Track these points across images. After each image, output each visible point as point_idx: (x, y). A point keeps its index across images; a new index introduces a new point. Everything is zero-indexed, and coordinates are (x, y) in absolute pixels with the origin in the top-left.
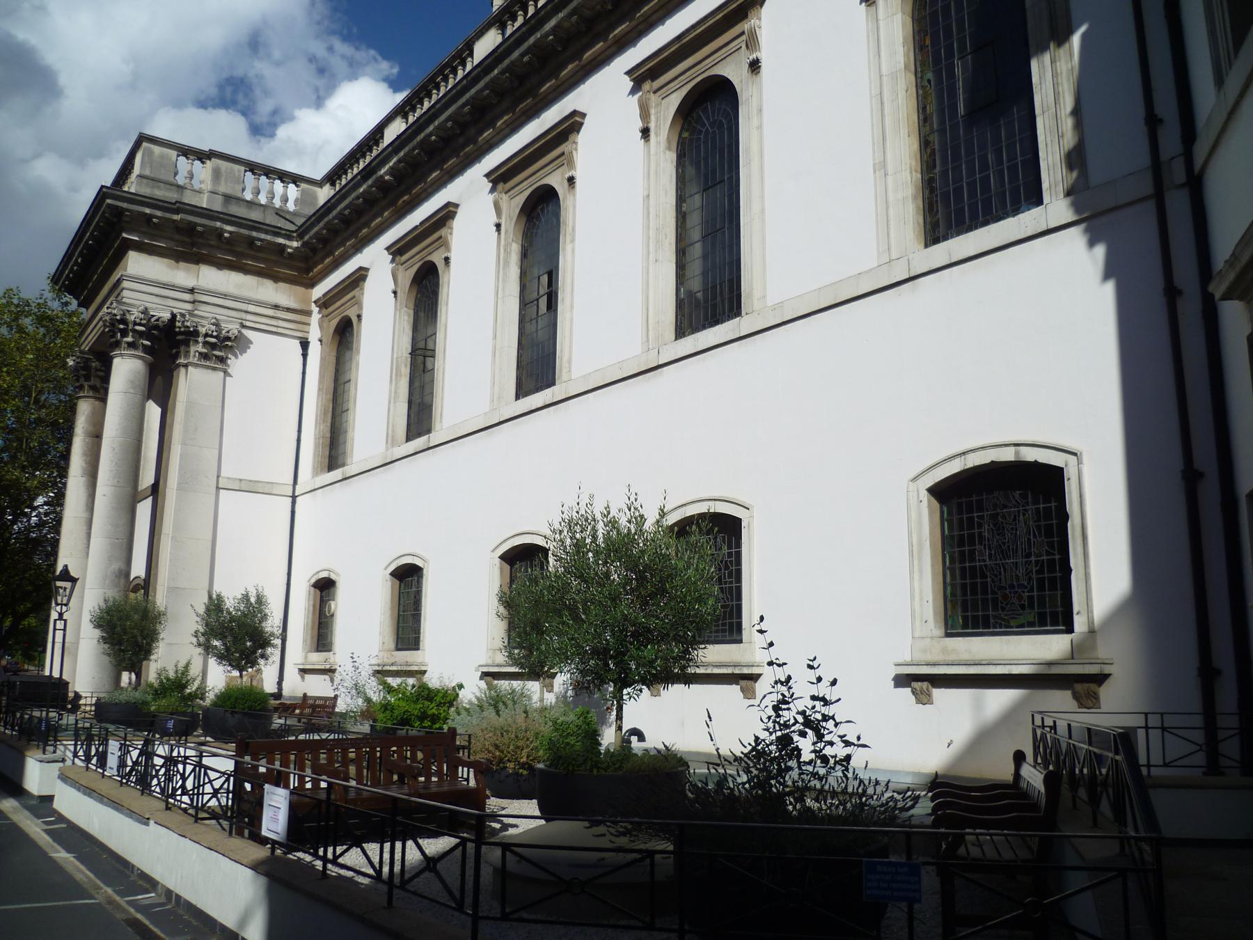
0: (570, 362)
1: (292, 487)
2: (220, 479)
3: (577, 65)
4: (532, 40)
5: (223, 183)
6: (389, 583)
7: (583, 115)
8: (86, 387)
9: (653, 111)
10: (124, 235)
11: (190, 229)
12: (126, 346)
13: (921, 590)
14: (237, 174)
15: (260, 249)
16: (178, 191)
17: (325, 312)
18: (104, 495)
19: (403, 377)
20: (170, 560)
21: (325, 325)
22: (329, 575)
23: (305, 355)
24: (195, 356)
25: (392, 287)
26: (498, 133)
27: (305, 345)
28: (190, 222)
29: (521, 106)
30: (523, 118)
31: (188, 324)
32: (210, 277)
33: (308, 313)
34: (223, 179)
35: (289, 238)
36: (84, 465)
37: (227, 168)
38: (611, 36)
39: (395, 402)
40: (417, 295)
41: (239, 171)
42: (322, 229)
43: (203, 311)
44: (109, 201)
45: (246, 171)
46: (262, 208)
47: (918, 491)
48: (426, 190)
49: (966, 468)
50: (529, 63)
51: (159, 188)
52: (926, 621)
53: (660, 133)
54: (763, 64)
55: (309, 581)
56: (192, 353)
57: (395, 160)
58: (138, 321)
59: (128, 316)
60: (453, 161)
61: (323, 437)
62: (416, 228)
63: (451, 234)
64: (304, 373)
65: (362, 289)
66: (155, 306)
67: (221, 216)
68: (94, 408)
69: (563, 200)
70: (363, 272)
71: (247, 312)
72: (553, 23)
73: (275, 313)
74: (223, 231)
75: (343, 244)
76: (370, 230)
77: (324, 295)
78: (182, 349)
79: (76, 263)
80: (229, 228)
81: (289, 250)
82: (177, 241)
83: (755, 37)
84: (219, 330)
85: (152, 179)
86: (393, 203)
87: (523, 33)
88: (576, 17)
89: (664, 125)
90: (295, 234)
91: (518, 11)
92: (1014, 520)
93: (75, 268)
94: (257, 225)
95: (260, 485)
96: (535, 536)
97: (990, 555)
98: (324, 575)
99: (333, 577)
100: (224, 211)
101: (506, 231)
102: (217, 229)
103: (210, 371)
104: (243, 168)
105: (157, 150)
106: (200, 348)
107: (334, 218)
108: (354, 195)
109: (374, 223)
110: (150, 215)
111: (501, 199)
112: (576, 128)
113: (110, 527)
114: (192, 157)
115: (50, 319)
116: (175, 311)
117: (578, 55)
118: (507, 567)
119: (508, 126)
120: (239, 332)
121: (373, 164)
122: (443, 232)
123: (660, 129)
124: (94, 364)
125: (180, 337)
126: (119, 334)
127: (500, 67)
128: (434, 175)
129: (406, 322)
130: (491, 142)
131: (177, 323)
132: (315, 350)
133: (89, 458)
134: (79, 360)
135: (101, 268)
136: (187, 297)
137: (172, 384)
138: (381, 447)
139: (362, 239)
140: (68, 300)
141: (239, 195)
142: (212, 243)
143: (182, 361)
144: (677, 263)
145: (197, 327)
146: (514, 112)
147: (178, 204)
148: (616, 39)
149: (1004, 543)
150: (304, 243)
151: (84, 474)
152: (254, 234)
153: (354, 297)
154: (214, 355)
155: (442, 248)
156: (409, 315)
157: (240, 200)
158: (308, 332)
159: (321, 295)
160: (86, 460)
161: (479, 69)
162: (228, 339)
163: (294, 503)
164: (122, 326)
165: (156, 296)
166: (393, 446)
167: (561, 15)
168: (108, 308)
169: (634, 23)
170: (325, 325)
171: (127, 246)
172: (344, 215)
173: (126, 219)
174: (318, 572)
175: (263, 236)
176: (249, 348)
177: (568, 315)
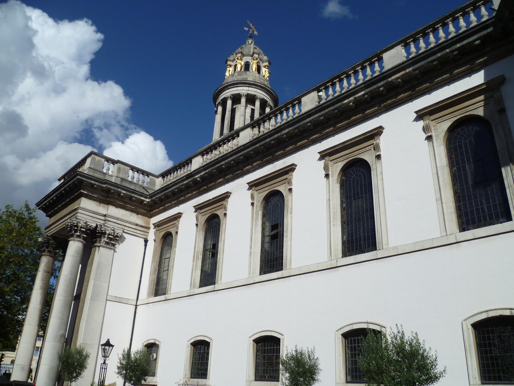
0: (291, 261)
1: (136, 301)
2: (108, 296)
3: (294, 147)
4: (276, 136)
5: (121, 173)
6: (190, 348)
7: (296, 166)
8: (46, 251)
9: (330, 168)
10: (82, 191)
11: (108, 191)
12: (76, 236)
13: (472, 365)
14: (127, 170)
15: (134, 201)
16: (103, 175)
17: (157, 228)
18: (60, 300)
19: (199, 259)
20: (84, 331)
21: (157, 234)
22: (155, 342)
23: (146, 246)
24: (103, 243)
25: (195, 222)
26: (253, 168)
27: (146, 241)
28: (109, 188)
29: (266, 159)
30: (266, 163)
31: (103, 229)
32: (113, 211)
33: (149, 228)
34: (121, 172)
35: (146, 197)
36: (41, 285)
37: (123, 168)
38: (311, 138)
39: (195, 270)
40: (206, 226)
41: (127, 169)
42: (162, 195)
43: (109, 224)
44: (79, 177)
45: (130, 169)
46: (135, 184)
47: (467, 324)
48: (215, 185)
49: (488, 317)
50: (273, 144)
51: (96, 173)
52: (475, 378)
53: (334, 176)
54: (382, 156)
55: (143, 344)
56: (102, 241)
57: (203, 173)
58: (83, 226)
59: (79, 224)
60: (230, 175)
61: (153, 281)
62: (210, 200)
63: (227, 204)
64: (145, 253)
65: (179, 221)
66: (90, 221)
67: (121, 187)
68: (49, 260)
69: (286, 197)
70: (180, 215)
71: (125, 226)
72: (287, 131)
73: (136, 227)
75: (170, 202)
76: (185, 198)
78: (98, 239)
79: (52, 199)
81: (145, 202)
82: (102, 195)
83: (378, 147)
84: (114, 233)
85: (94, 169)
86: (199, 189)
87: (273, 133)
88: (297, 130)
89: (335, 173)
90: (148, 196)
91: (261, 123)
92: (509, 338)
93: (51, 201)
94: (135, 191)
95: (123, 299)
96: (272, 332)
97: (499, 352)
98: (153, 341)
99: (157, 342)
100: (121, 184)
101: (256, 206)
102: (119, 191)
103: (109, 249)
104: (129, 168)
105: (97, 158)
106: (106, 239)
107: (169, 192)
108: (180, 184)
109: (187, 196)
110: (94, 184)
111: (254, 193)
113: (61, 314)
114: (110, 162)
115: (23, 219)
116: (98, 223)
117: (295, 143)
118: (255, 345)
119: (258, 165)
120: (122, 234)
121: (193, 173)
122: (223, 202)
123: (334, 175)
124: (51, 241)
125: (97, 234)
126: (73, 231)
128: (220, 180)
129: (202, 237)
130: (249, 170)
131: (98, 228)
132: (151, 244)
133: (44, 282)
134: (46, 239)
135: (65, 202)
136: (103, 218)
137: (91, 253)
139: (180, 201)
140: (32, 212)
141: (127, 179)
142: (115, 197)
143: (98, 244)
144: (341, 226)
145: (106, 231)
147: (105, 181)
148: (312, 139)
149: (505, 347)
150: (152, 200)
151: (41, 289)
152: (133, 195)
153: (175, 224)
154: (111, 243)
155: (222, 209)
156: (203, 235)
157: (127, 181)
158: (148, 236)
159: (157, 222)
160: (42, 282)
161: (250, 143)
162: (117, 236)
163: (136, 308)
164: (76, 228)
165: (91, 216)
166: (194, 288)
167: (290, 129)
168: (70, 220)
169: (321, 135)
170: (157, 234)
171: (81, 195)
172: (175, 191)
173: (84, 185)
174: (149, 340)
175: (136, 196)
176: (124, 241)
177: (289, 243)
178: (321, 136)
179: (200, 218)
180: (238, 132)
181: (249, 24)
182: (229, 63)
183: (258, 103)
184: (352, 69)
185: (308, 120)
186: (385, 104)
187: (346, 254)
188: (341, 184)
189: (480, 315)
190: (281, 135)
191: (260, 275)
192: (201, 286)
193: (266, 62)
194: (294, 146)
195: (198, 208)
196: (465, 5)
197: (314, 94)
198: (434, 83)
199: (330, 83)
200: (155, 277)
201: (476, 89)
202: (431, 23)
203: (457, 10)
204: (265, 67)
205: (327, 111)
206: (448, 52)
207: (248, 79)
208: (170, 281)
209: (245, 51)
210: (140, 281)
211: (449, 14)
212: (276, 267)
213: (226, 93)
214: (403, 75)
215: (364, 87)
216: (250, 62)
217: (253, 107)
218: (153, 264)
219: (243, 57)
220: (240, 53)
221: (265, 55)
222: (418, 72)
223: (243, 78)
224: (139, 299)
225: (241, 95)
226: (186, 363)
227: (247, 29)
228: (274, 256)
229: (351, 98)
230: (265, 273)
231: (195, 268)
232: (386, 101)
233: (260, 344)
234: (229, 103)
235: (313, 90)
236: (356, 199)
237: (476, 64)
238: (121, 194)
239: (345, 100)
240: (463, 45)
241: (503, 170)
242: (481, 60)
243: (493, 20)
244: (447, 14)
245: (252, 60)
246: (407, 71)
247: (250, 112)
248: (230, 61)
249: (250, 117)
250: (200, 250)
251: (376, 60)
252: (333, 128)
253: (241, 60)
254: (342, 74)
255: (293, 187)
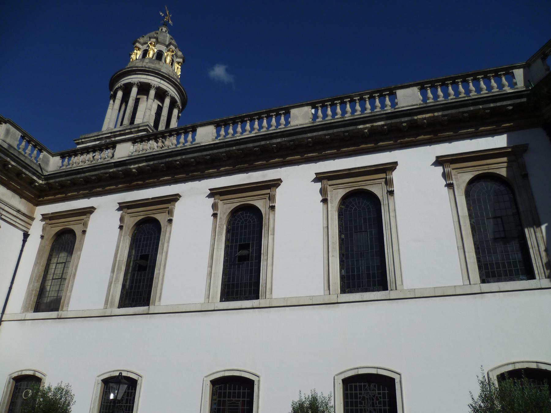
4: (263, 143)
5: (9, 137)
6: (100, 385)
9: (329, 193)
14: (17, 136)
17: (48, 221)
19: (122, 271)
23: (24, 241)
26: (217, 172)
27: (26, 236)
29: (240, 166)
33: (32, 219)
34: (10, 135)
35: (39, 178)
38: (306, 155)
40: (134, 231)
46: (24, 157)
47: (493, 376)
53: (333, 203)
61: (36, 290)
64: (22, 251)
65: (89, 218)
70: (93, 210)
72: (279, 140)
73: (17, 214)
74: (9, 163)
76: (103, 190)
77: (52, 213)
80: (13, 163)
83: (392, 182)
89: (335, 200)
90: (43, 177)
91: (231, 124)
94: (27, 166)
96: (242, 372)
98: (31, 373)
99: (38, 375)
101: (220, 218)
102: (7, 161)
107: (81, 178)
108: (102, 171)
109: (109, 188)
112: (277, 186)
127: (238, 147)
128: (166, 178)
129: (127, 243)
138: (102, 306)
139: (93, 193)
146: (234, 167)
152: (24, 170)
155: (165, 213)
156: (129, 240)
158: (29, 229)
161: (225, 144)
169: (320, 155)
175: (27, 173)
178: (319, 156)
179: (127, 218)
180: (195, 126)
181: (166, 10)
182: (138, 45)
183: (167, 101)
184: (359, 95)
185: (309, 135)
186: (402, 140)
187: (345, 290)
188: (339, 212)
189: (506, 367)
190: (270, 143)
191: (220, 302)
192: (121, 306)
193: (180, 58)
194: (282, 159)
195: (123, 206)
196: (488, 70)
197: (309, 111)
198: (457, 134)
199: (330, 103)
200: (38, 285)
201: (501, 150)
202: (452, 76)
203: (480, 72)
204: (178, 63)
205: (335, 130)
206: (481, 108)
207: (162, 70)
208: (68, 294)
209: (161, 38)
210: (10, 288)
211: (472, 73)
212: (245, 294)
213: (132, 78)
214: (430, 117)
215: (385, 117)
216: (164, 52)
217: (161, 104)
218: (37, 268)
219: (157, 44)
220: (155, 38)
221: (179, 50)
222: (446, 119)
223: (155, 67)
224: (6, 312)
225: (151, 85)
226: (92, 405)
227: (163, 15)
228: (233, 281)
229: (368, 125)
230: (227, 300)
231: (115, 281)
232: (404, 137)
233: (217, 386)
234: (135, 90)
235: (307, 105)
236: (358, 232)
237: (502, 127)
238: (8, 165)
239: (360, 125)
240: (496, 106)
241: (526, 230)
242: (507, 125)
243: (529, 92)
244: (470, 73)
245: (167, 51)
246: (436, 114)
247: (157, 108)
248: (140, 43)
249: (155, 113)
250: (124, 260)
251: (387, 94)
252: (336, 151)
253: (154, 46)
254: (347, 97)
255: (277, 205)
